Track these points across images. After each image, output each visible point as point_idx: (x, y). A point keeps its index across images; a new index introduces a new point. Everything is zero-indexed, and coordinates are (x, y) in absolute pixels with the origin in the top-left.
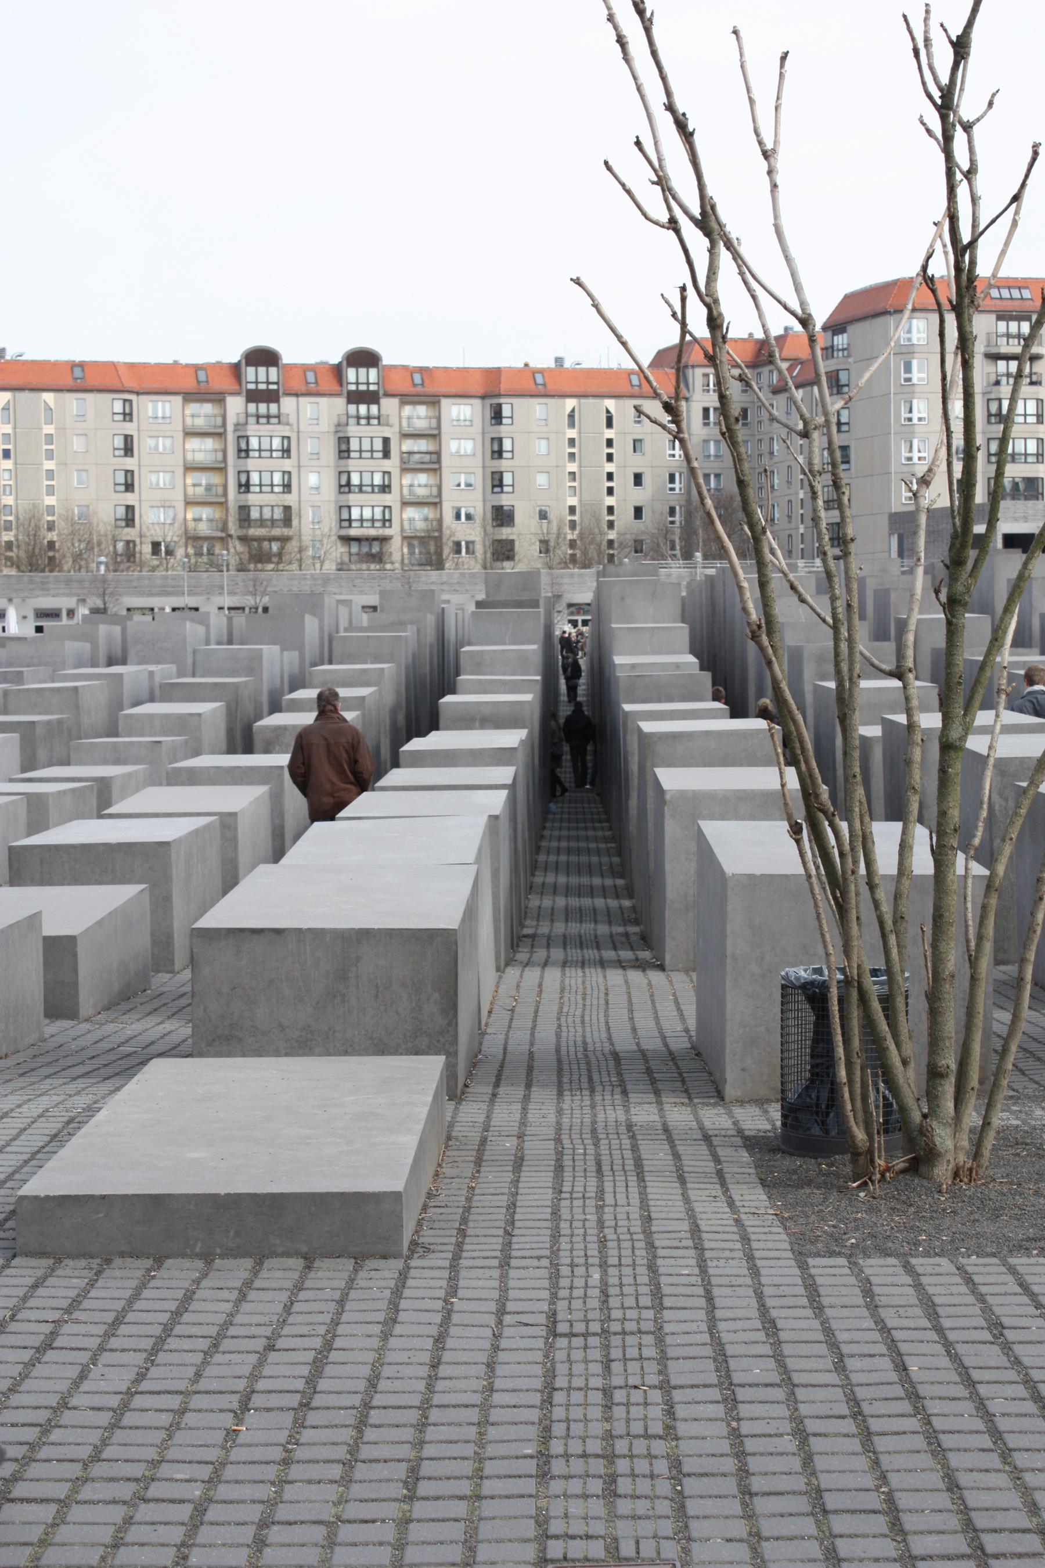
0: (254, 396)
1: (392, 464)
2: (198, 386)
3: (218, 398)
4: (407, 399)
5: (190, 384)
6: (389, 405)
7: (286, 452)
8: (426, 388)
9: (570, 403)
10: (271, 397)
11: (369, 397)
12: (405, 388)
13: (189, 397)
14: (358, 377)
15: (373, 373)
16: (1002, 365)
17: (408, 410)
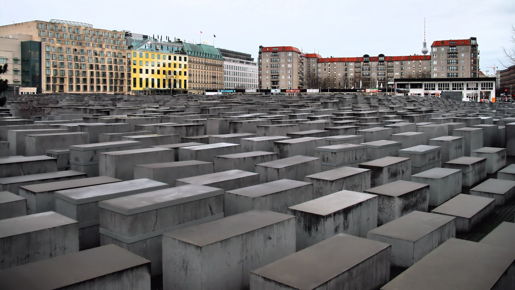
0: (365, 62)
1: (386, 72)
2: (357, 60)
3: (360, 62)
4: (388, 62)
5: (355, 60)
6: (385, 63)
7: (369, 70)
8: (391, 59)
9: (414, 61)
10: (367, 62)
11: (382, 61)
12: (388, 60)
13: (356, 62)
14: (382, 59)
15: (383, 58)
16: (450, 55)
17: (390, 63)
